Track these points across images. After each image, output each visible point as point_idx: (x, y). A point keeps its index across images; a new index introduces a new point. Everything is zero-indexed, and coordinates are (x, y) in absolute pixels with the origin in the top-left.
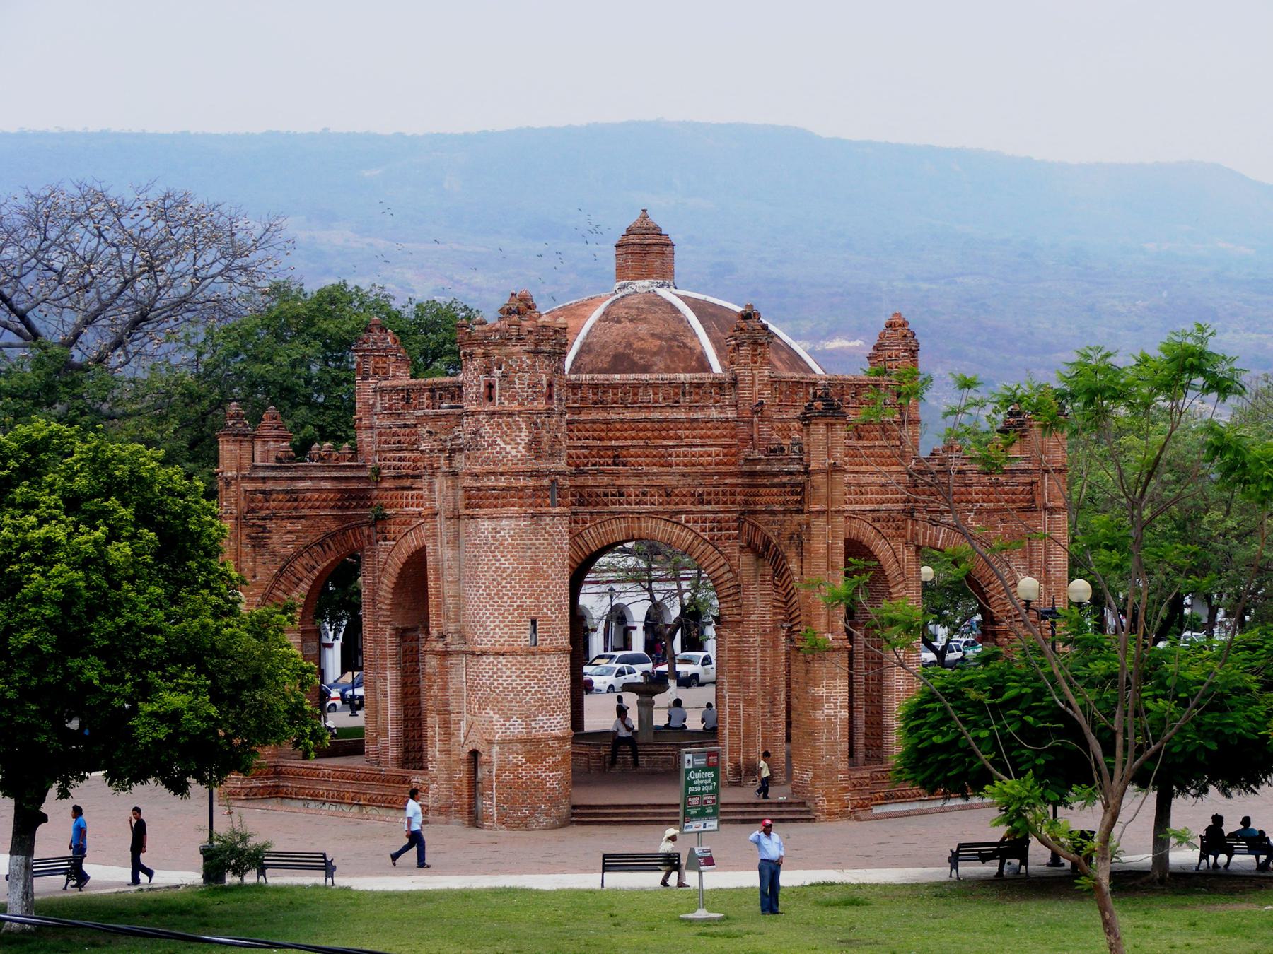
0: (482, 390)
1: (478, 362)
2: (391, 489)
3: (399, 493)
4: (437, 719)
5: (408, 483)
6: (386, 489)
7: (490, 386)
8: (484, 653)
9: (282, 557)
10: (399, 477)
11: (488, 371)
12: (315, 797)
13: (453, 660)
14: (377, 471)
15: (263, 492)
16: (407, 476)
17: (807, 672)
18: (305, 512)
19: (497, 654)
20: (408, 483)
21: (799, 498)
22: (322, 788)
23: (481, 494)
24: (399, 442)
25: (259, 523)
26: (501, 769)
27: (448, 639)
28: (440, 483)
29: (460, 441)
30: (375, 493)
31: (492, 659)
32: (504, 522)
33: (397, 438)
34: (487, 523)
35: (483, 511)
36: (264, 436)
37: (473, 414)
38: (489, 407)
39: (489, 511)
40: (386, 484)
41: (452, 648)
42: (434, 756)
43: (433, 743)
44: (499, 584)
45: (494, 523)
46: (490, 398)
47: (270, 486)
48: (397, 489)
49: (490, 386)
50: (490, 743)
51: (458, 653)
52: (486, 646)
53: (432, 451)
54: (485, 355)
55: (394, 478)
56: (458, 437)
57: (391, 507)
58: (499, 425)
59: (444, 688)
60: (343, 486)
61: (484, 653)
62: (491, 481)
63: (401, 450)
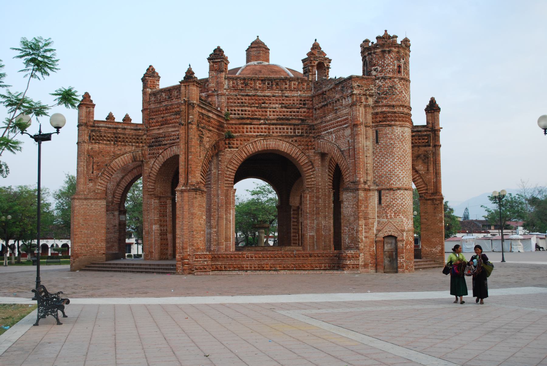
0: (396, 67)
1: (393, 55)
2: (236, 124)
3: (241, 126)
4: (364, 222)
5: (248, 122)
6: (233, 124)
7: (399, 67)
8: (399, 189)
9: (206, 149)
10: (243, 119)
11: (399, 60)
12: (241, 269)
13: (371, 193)
14: (227, 115)
15: (203, 114)
16: (248, 118)
17: (435, 209)
18: (211, 128)
19: (406, 189)
20: (248, 122)
21: (426, 141)
22: (245, 264)
23: (397, 115)
24: (242, 103)
25: (202, 130)
26: (406, 244)
27: (369, 183)
28: (362, 109)
29: (373, 91)
30: (225, 125)
31: (402, 191)
32: (406, 129)
33: (239, 101)
34: (399, 128)
35: (398, 123)
36: (87, 104)
37: (390, 78)
38: (399, 76)
39: (401, 123)
40: (231, 122)
41: (372, 188)
42: (362, 240)
43: (362, 234)
44: (405, 157)
45: (402, 129)
46: (399, 72)
47: (203, 111)
48: (240, 124)
49: (399, 67)
50: (403, 231)
51: (373, 190)
52: (399, 185)
53: (359, 94)
54: (398, 52)
55: (238, 119)
56: (372, 90)
57: (236, 132)
58: (404, 85)
59: (367, 207)
60: (220, 119)
61: (399, 189)
62: (401, 109)
63: (244, 106)
